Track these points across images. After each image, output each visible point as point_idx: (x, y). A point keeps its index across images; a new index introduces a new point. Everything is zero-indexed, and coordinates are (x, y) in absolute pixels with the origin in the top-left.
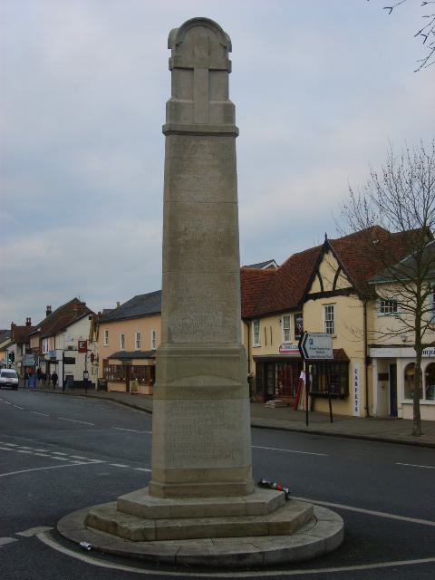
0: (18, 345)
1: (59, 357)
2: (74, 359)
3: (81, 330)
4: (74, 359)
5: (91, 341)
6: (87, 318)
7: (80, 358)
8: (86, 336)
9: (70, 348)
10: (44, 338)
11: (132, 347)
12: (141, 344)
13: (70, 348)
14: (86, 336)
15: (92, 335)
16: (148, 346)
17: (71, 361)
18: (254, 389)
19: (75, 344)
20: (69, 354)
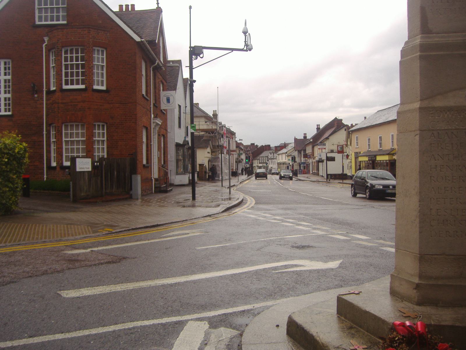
0: (298, 151)
1: (324, 158)
2: (334, 158)
3: (340, 137)
4: (334, 158)
5: (347, 145)
6: (343, 129)
7: (338, 157)
8: (343, 142)
9: (332, 151)
10: (316, 145)
11: (375, 147)
12: (359, 144)
13: (332, 151)
14: (343, 142)
15: (347, 142)
16: (388, 146)
17: (333, 159)
18: (391, 161)
19: (335, 148)
20: (329, 155)
